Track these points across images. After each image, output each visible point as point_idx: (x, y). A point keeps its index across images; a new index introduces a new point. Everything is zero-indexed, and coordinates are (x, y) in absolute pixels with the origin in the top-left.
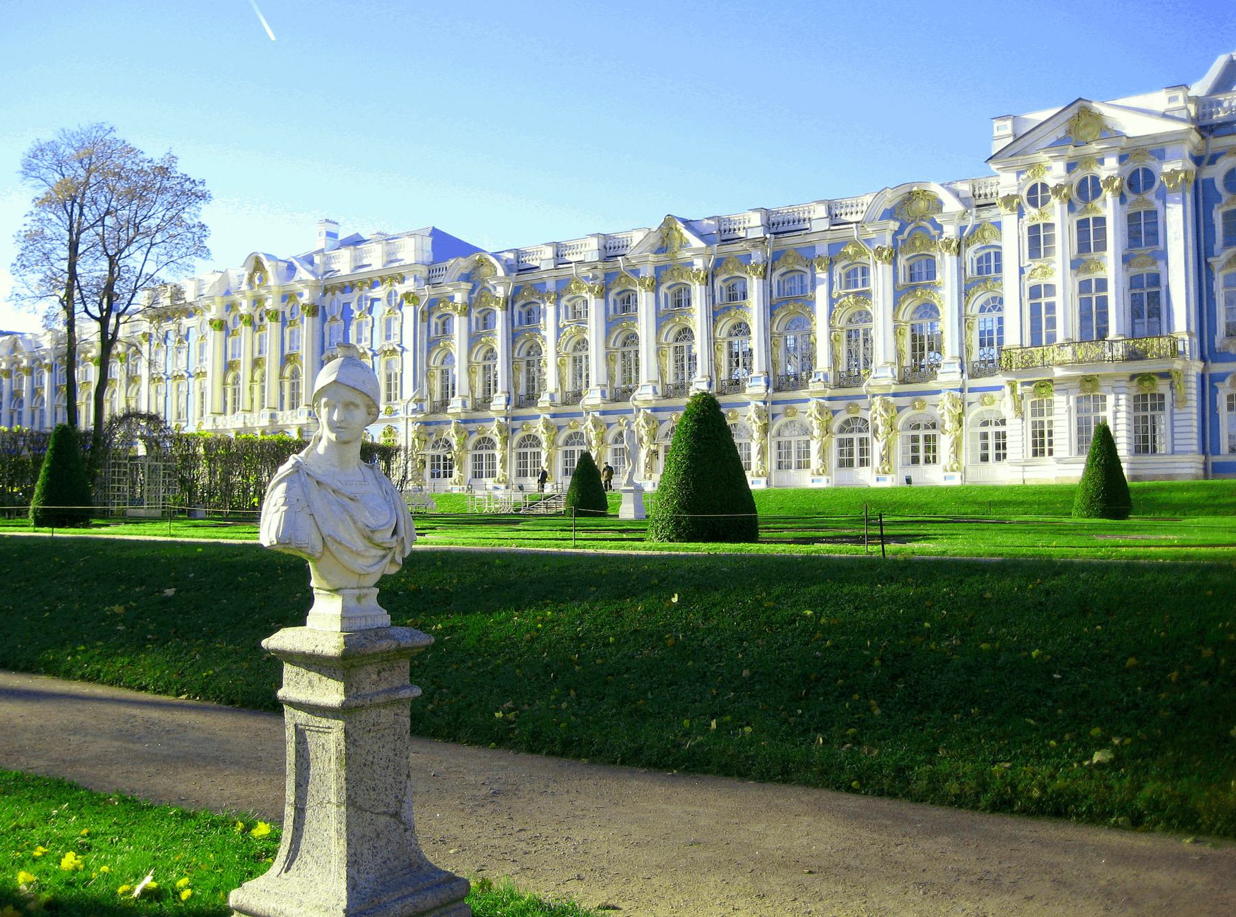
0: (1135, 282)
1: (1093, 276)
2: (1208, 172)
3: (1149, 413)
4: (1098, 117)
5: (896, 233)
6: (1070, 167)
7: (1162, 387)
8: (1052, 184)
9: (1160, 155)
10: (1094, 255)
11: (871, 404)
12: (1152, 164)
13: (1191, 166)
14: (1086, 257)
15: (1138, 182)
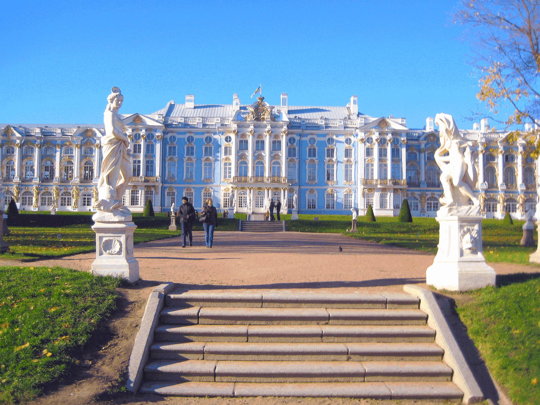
0: (147, 162)
1: (137, 160)
2: (166, 136)
3: (149, 196)
4: (141, 119)
5: (82, 141)
6: (133, 130)
7: (153, 189)
8: (128, 134)
9: (156, 131)
10: (137, 154)
11: (72, 188)
12: (153, 132)
13: (162, 135)
14: (135, 154)
15: (149, 137)
